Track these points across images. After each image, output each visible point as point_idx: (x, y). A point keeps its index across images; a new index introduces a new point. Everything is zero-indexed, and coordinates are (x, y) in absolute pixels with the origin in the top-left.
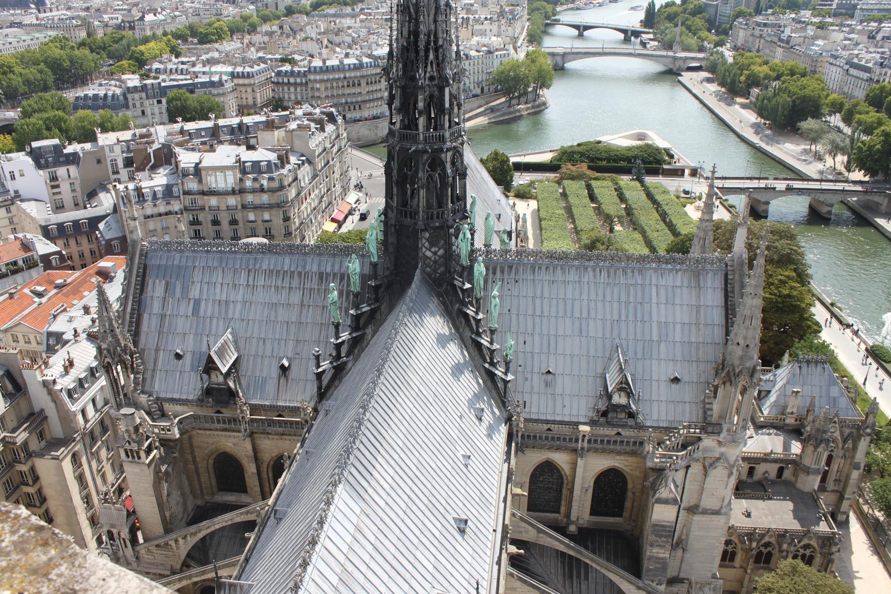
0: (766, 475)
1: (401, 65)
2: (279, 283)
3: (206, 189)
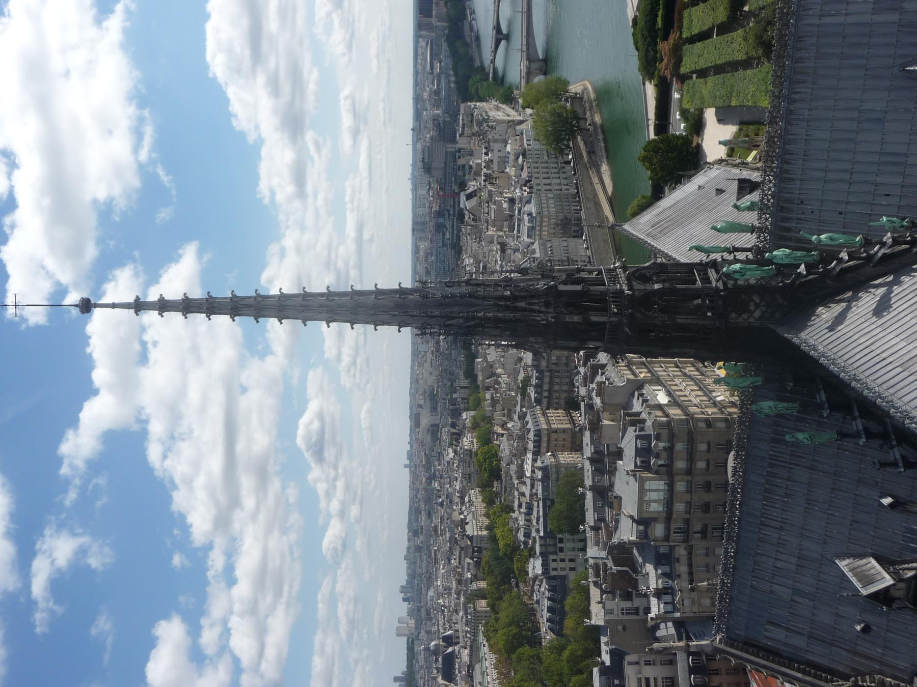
1: (531, 339)
3: (665, 515)
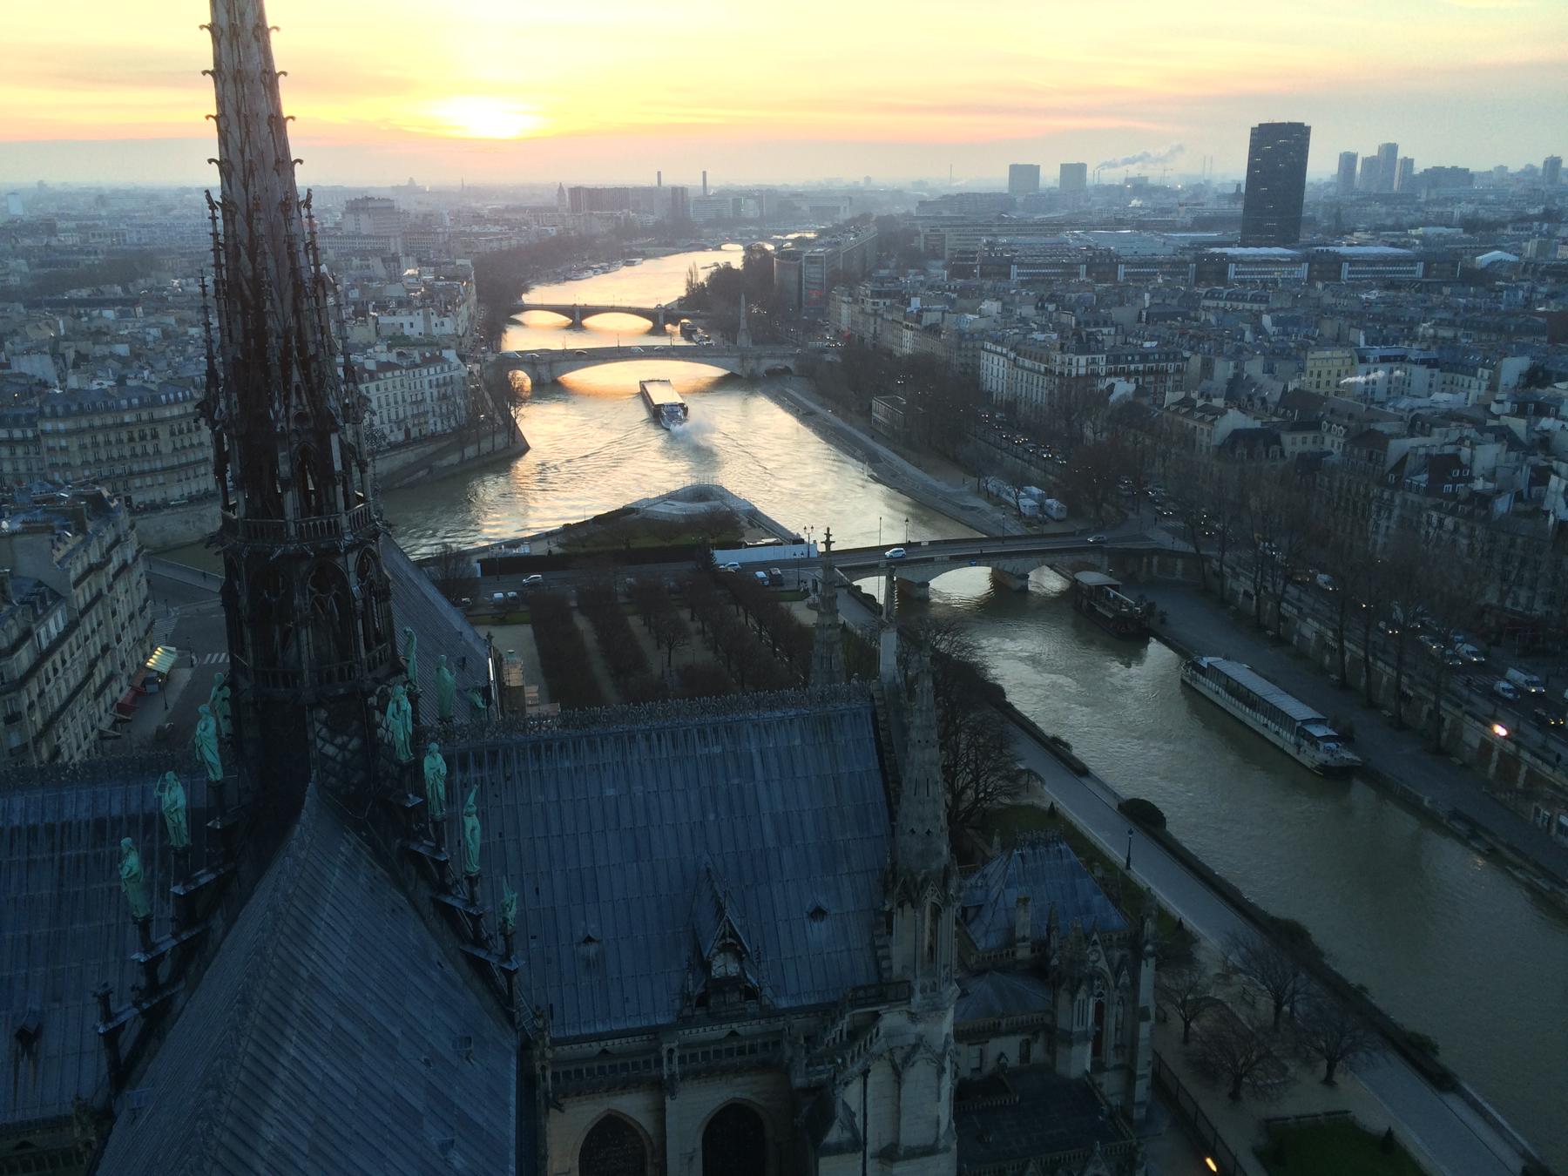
0: (1003, 1060)
1: (235, 397)
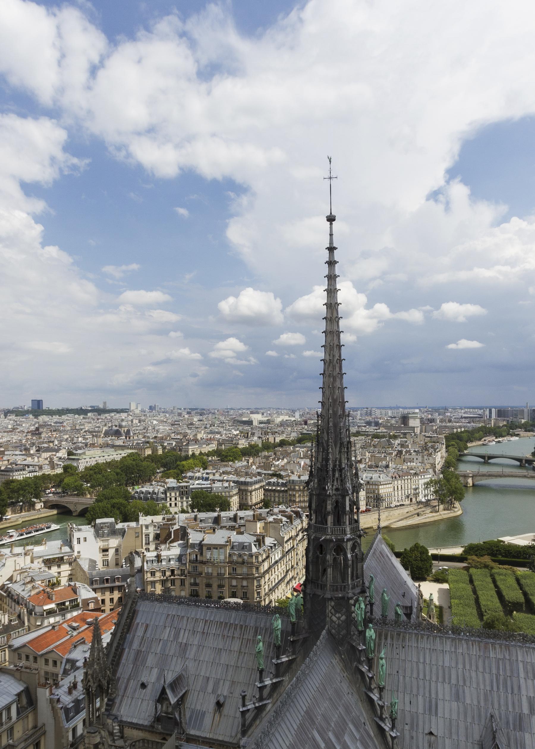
1: (316, 481)
2: (226, 633)
